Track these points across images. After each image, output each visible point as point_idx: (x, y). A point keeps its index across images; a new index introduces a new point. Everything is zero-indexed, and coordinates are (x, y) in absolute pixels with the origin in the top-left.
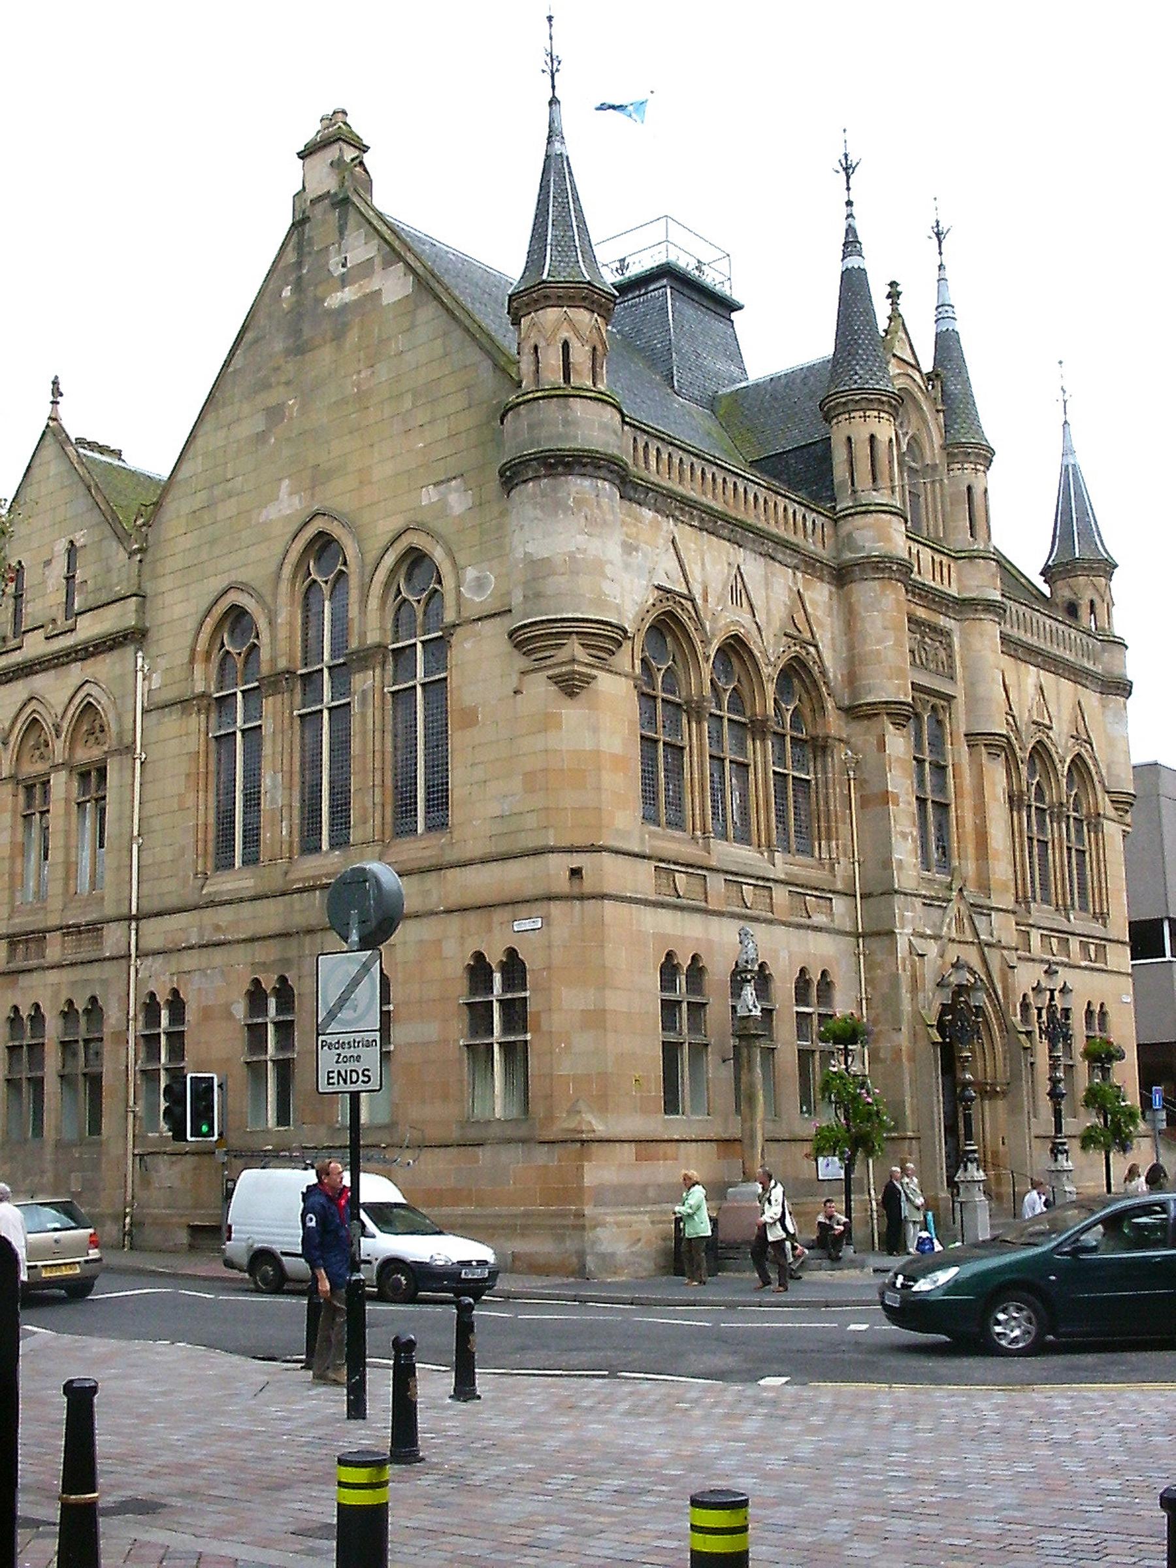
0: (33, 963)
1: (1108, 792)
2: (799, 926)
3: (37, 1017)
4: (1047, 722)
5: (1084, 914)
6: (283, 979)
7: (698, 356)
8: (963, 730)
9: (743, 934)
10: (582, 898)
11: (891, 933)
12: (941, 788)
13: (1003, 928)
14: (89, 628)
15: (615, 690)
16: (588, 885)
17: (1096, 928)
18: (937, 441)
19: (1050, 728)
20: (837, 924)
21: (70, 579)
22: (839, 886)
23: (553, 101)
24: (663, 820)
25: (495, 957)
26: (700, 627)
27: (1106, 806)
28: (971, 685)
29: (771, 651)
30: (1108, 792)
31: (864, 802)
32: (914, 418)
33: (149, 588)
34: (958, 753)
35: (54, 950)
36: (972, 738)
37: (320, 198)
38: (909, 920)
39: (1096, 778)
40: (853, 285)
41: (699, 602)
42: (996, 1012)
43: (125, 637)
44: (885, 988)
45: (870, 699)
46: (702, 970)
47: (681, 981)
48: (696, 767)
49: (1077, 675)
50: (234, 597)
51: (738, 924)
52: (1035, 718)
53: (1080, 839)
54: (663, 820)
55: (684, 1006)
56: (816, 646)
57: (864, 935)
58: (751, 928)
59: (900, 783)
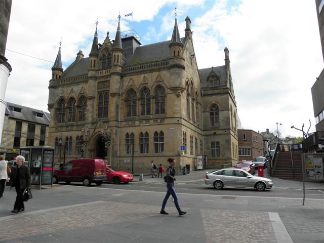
1: (169, 89)
23: (60, 48)
27: (169, 91)
30: (169, 89)
39: (165, 87)
40: (95, 39)
49: (159, 70)
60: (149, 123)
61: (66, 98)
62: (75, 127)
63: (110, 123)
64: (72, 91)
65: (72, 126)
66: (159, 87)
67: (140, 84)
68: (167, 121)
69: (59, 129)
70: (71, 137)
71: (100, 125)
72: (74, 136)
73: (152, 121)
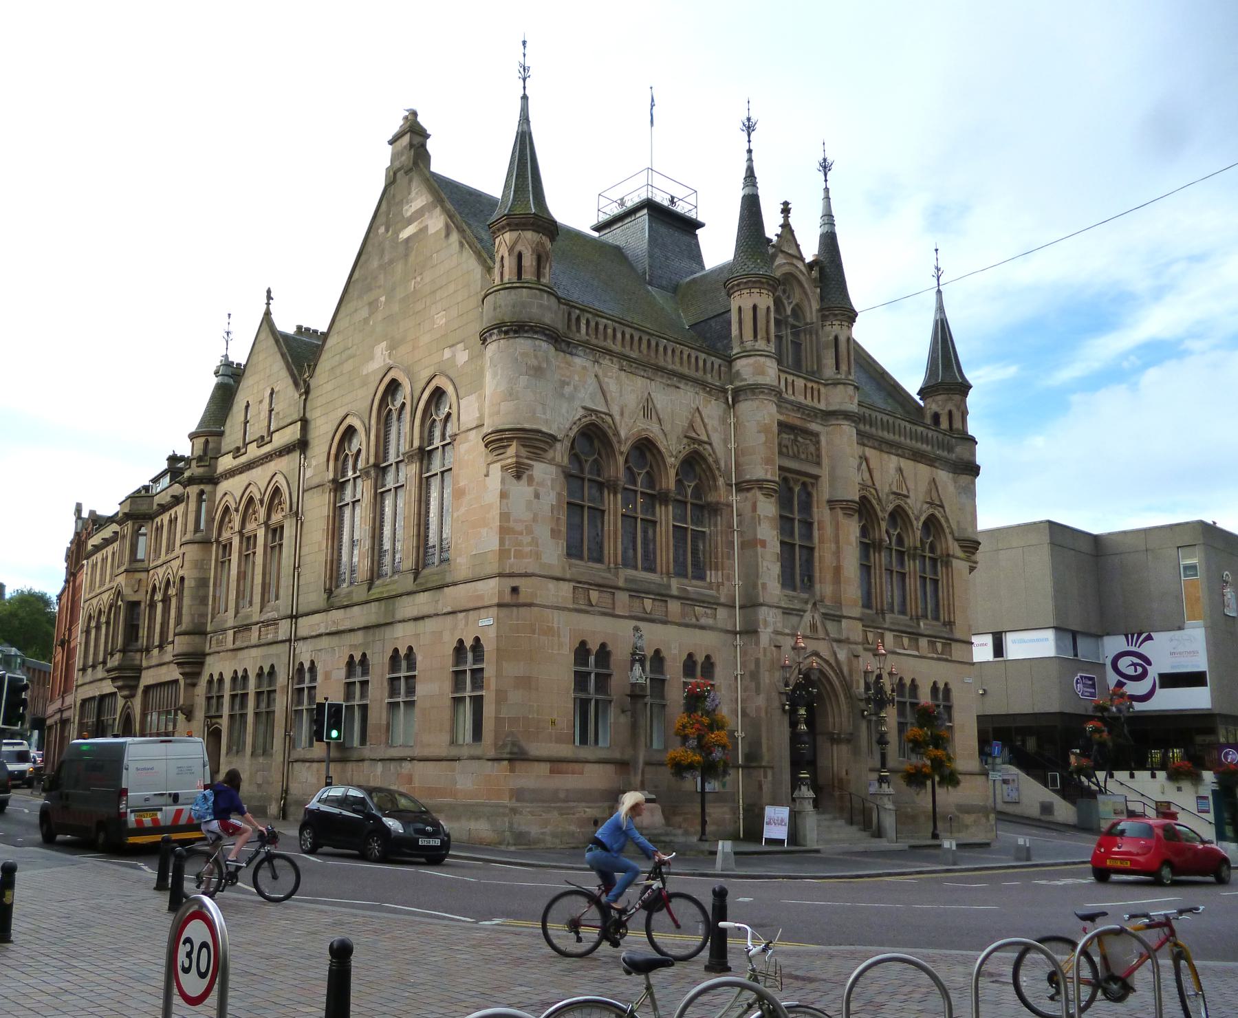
0: (245, 644)
2: (687, 626)
3: (245, 677)
4: (905, 492)
5: (934, 623)
6: (364, 655)
7: (667, 258)
8: (826, 497)
9: (637, 629)
10: (518, 605)
11: (755, 632)
12: (809, 536)
13: (852, 629)
14: (279, 440)
15: (544, 472)
16: (522, 598)
17: (945, 632)
18: (815, 306)
19: (907, 497)
20: (720, 625)
21: (271, 411)
22: (723, 600)
24: (586, 556)
25: (468, 643)
26: (617, 434)
27: (955, 549)
28: (833, 469)
29: (672, 448)
31: (743, 546)
32: (797, 291)
33: (308, 415)
34: (821, 513)
35: (254, 635)
36: (832, 503)
37: (399, 169)
38: (769, 620)
39: (947, 531)
41: (617, 418)
42: (842, 686)
43: (294, 446)
44: (752, 667)
45: (748, 477)
46: (608, 654)
47: (592, 659)
48: (613, 523)
49: (931, 461)
50: (349, 421)
51: (634, 623)
52: (895, 489)
53: (936, 573)
54: (586, 556)
55: (593, 676)
56: (710, 444)
57: (740, 633)
58: (641, 624)
59: (769, 534)
60: (918, 649)
61: (623, 434)
62: (674, 607)
63: (844, 622)
64: (648, 409)
65: (663, 596)
66: (932, 525)
67: (887, 489)
68: (957, 651)
69: (594, 595)
70: (657, 652)
71: (813, 627)
72: (675, 652)
73: (923, 642)
